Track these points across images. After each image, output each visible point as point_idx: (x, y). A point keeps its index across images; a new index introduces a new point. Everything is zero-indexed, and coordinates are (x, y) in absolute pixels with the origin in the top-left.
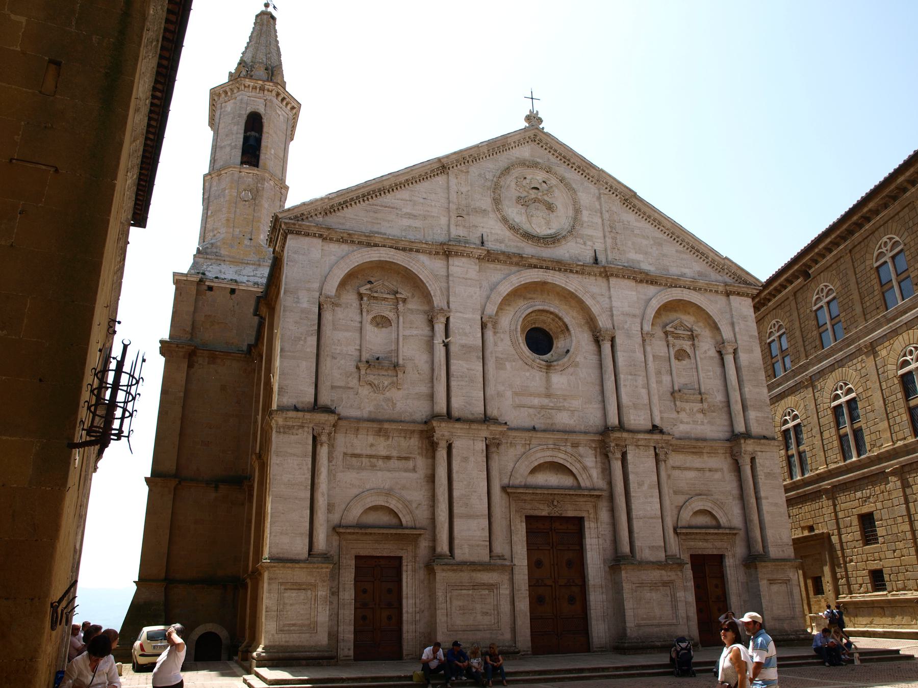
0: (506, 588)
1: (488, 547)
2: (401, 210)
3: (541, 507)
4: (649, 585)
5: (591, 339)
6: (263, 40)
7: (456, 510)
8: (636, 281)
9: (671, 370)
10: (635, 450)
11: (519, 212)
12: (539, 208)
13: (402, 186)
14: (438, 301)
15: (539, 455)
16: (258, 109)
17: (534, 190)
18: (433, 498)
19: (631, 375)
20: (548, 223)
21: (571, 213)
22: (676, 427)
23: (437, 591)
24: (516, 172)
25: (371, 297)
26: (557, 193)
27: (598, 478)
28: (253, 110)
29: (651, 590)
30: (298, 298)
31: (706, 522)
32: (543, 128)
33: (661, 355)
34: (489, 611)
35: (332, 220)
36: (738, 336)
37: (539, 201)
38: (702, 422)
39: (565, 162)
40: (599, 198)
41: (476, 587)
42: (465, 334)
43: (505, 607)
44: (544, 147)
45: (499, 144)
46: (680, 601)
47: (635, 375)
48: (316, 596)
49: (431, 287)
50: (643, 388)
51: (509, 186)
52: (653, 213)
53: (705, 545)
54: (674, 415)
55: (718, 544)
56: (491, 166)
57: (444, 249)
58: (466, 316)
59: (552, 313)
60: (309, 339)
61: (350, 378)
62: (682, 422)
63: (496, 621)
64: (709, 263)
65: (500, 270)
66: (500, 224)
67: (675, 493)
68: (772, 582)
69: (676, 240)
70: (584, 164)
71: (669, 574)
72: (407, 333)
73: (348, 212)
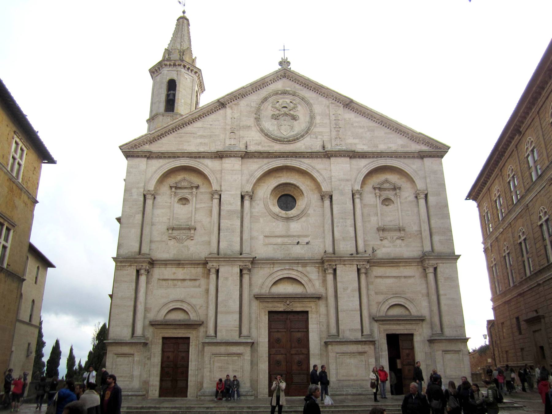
0: (248, 356)
1: (238, 331)
2: (196, 134)
3: (279, 305)
4: (349, 354)
5: (319, 198)
6: (179, 35)
7: (219, 309)
8: (351, 158)
9: (377, 213)
10: (343, 267)
11: (273, 124)
12: (286, 119)
13: (197, 119)
14: (215, 187)
15: (279, 273)
16: (173, 77)
17: (284, 109)
18: (207, 303)
19: (342, 219)
20: (292, 128)
21: (308, 119)
22: (380, 250)
23: (205, 357)
24: (270, 100)
25: (176, 188)
26: (299, 108)
27: (319, 286)
28: (170, 78)
29: (350, 357)
30: (131, 193)
31: (401, 312)
32: (290, 69)
33: (370, 203)
34: (237, 369)
35: (155, 148)
36: (428, 186)
37: (286, 114)
38: (400, 245)
39: (305, 87)
40: (328, 107)
41: (230, 355)
42: (230, 204)
43: (247, 367)
44: (292, 80)
45: (259, 84)
46: (371, 364)
47: (345, 219)
48: (134, 360)
49: (211, 178)
50: (351, 227)
51: (266, 109)
52: (367, 110)
53: (398, 327)
54: (379, 242)
55: (409, 327)
56: (254, 99)
57: (218, 155)
58: (230, 193)
59: (292, 184)
60: (137, 216)
61: (163, 236)
62: (384, 247)
63: (241, 376)
64: (410, 138)
65: (257, 162)
66: (258, 133)
67: (376, 293)
68: (446, 352)
69: (385, 126)
70: (317, 86)
71: (363, 347)
72: (198, 206)
73: (164, 140)
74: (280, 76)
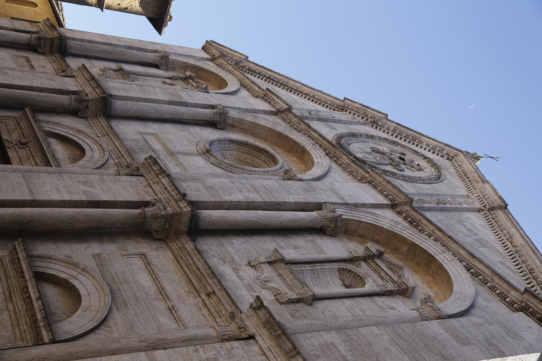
74: (445, 152)
